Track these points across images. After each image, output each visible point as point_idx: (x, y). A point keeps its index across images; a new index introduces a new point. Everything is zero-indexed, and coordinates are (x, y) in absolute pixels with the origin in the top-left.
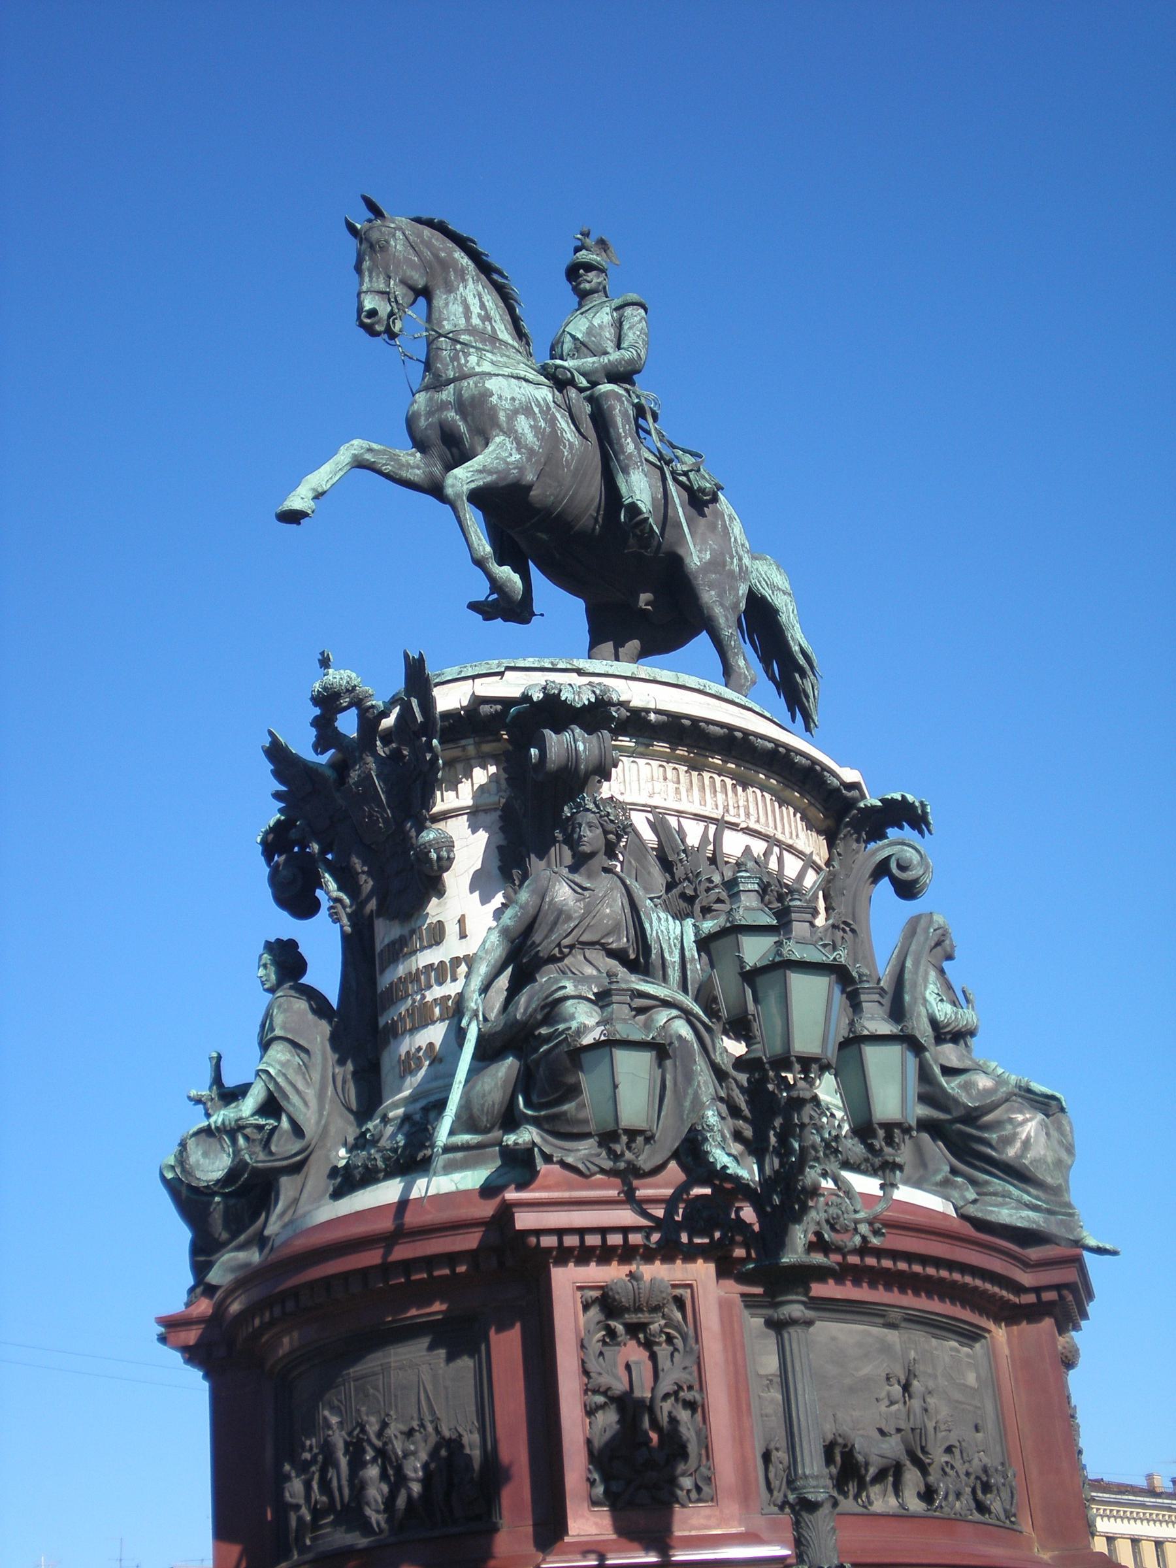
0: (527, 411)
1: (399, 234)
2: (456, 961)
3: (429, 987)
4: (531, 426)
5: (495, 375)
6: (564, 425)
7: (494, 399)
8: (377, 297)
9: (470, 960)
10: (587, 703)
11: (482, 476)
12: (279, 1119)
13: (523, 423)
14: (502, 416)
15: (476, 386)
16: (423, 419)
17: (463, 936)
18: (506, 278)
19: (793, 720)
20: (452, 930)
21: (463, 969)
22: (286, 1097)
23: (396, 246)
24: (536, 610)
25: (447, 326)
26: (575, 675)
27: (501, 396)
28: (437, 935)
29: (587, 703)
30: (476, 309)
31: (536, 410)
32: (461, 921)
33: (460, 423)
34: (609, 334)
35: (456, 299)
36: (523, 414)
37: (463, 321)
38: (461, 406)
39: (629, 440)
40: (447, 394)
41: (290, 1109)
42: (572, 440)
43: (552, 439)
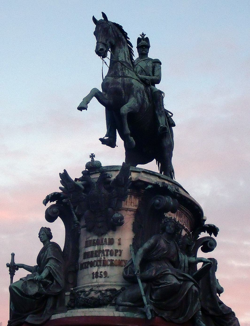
0: (139, 91)
2: (117, 251)
3: (107, 255)
5: (133, 78)
6: (146, 97)
9: (121, 251)
12: (53, 282)
16: (110, 85)
17: (119, 244)
18: (132, 47)
20: (116, 241)
21: (118, 253)
22: (56, 276)
25: (120, 59)
26: (158, 178)
28: (111, 242)
30: (127, 56)
32: (119, 240)
33: (123, 91)
34: (151, 69)
38: (123, 85)
40: (120, 80)
41: (57, 279)
43: (143, 100)
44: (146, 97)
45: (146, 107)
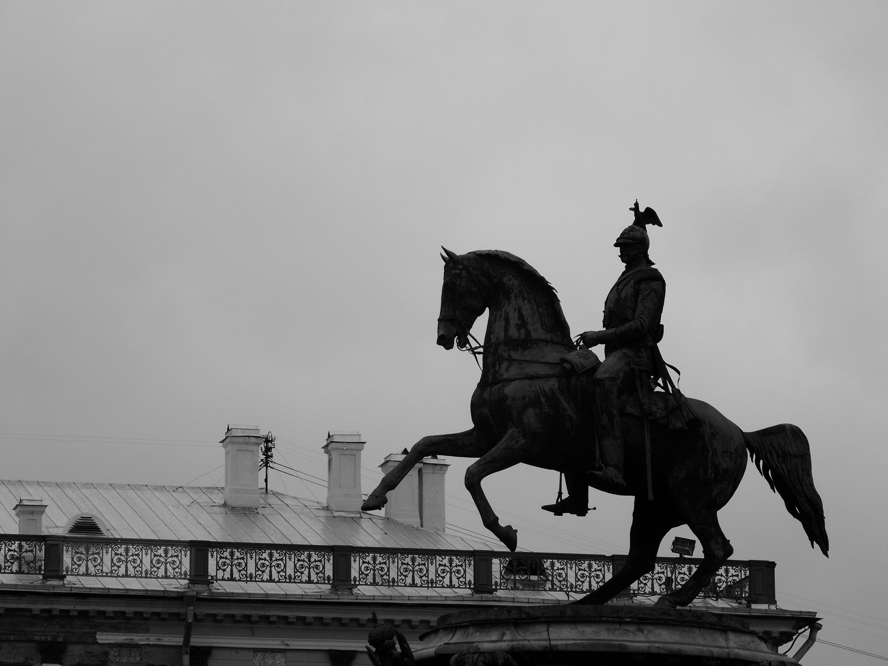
0: (535, 402)
1: (464, 273)
6: (566, 405)
7: (509, 402)
8: (448, 323)
15: (498, 393)
19: (813, 548)
23: (460, 284)
24: (590, 505)
27: (514, 398)
31: (543, 400)
33: (490, 419)
35: (501, 315)
37: (502, 334)
39: (604, 416)
40: (486, 395)
44: (566, 405)
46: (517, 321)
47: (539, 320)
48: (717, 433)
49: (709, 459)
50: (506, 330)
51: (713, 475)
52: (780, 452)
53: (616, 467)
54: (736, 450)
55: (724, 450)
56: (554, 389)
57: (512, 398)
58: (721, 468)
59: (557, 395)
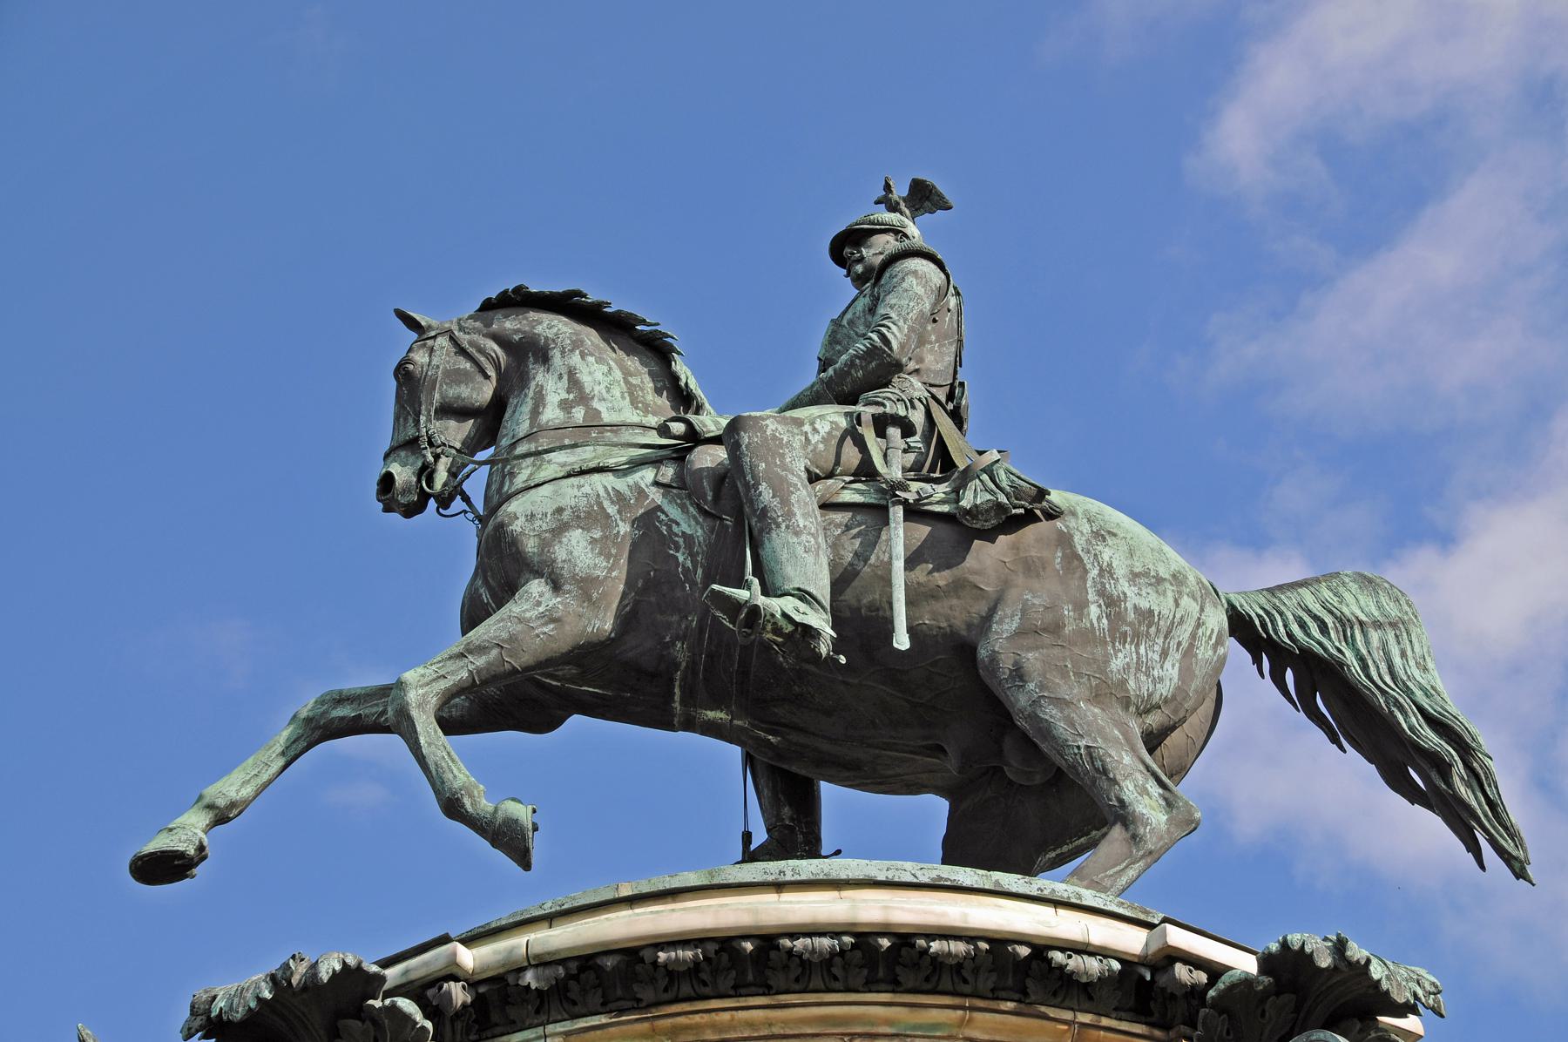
0: (591, 517)
1: (443, 341)
4: (593, 541)
10: (253, 1004)
11: (466, 660)
13: (574, 542)
14: (530, 546)
19: (1482, 867)
27: (532, 515)
29: (253, 1004)
31: (611, 510)
36: (579, 527)
42: (689, 532)
45: (689, 564)
46: (564, 395)
47: (626, 395)
48: (1109, 533)
49: (1089, 584)
50: (535, 413)
51: (1105, 621)
52: (1329, 620)
53: (804, 595)
54: (1174, 576)
55: (1137, 570)
56: (643, 486)
57: (526, 516)
58: (1129, 605)
59: (651, 496)
